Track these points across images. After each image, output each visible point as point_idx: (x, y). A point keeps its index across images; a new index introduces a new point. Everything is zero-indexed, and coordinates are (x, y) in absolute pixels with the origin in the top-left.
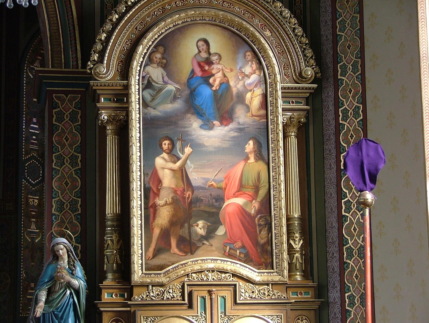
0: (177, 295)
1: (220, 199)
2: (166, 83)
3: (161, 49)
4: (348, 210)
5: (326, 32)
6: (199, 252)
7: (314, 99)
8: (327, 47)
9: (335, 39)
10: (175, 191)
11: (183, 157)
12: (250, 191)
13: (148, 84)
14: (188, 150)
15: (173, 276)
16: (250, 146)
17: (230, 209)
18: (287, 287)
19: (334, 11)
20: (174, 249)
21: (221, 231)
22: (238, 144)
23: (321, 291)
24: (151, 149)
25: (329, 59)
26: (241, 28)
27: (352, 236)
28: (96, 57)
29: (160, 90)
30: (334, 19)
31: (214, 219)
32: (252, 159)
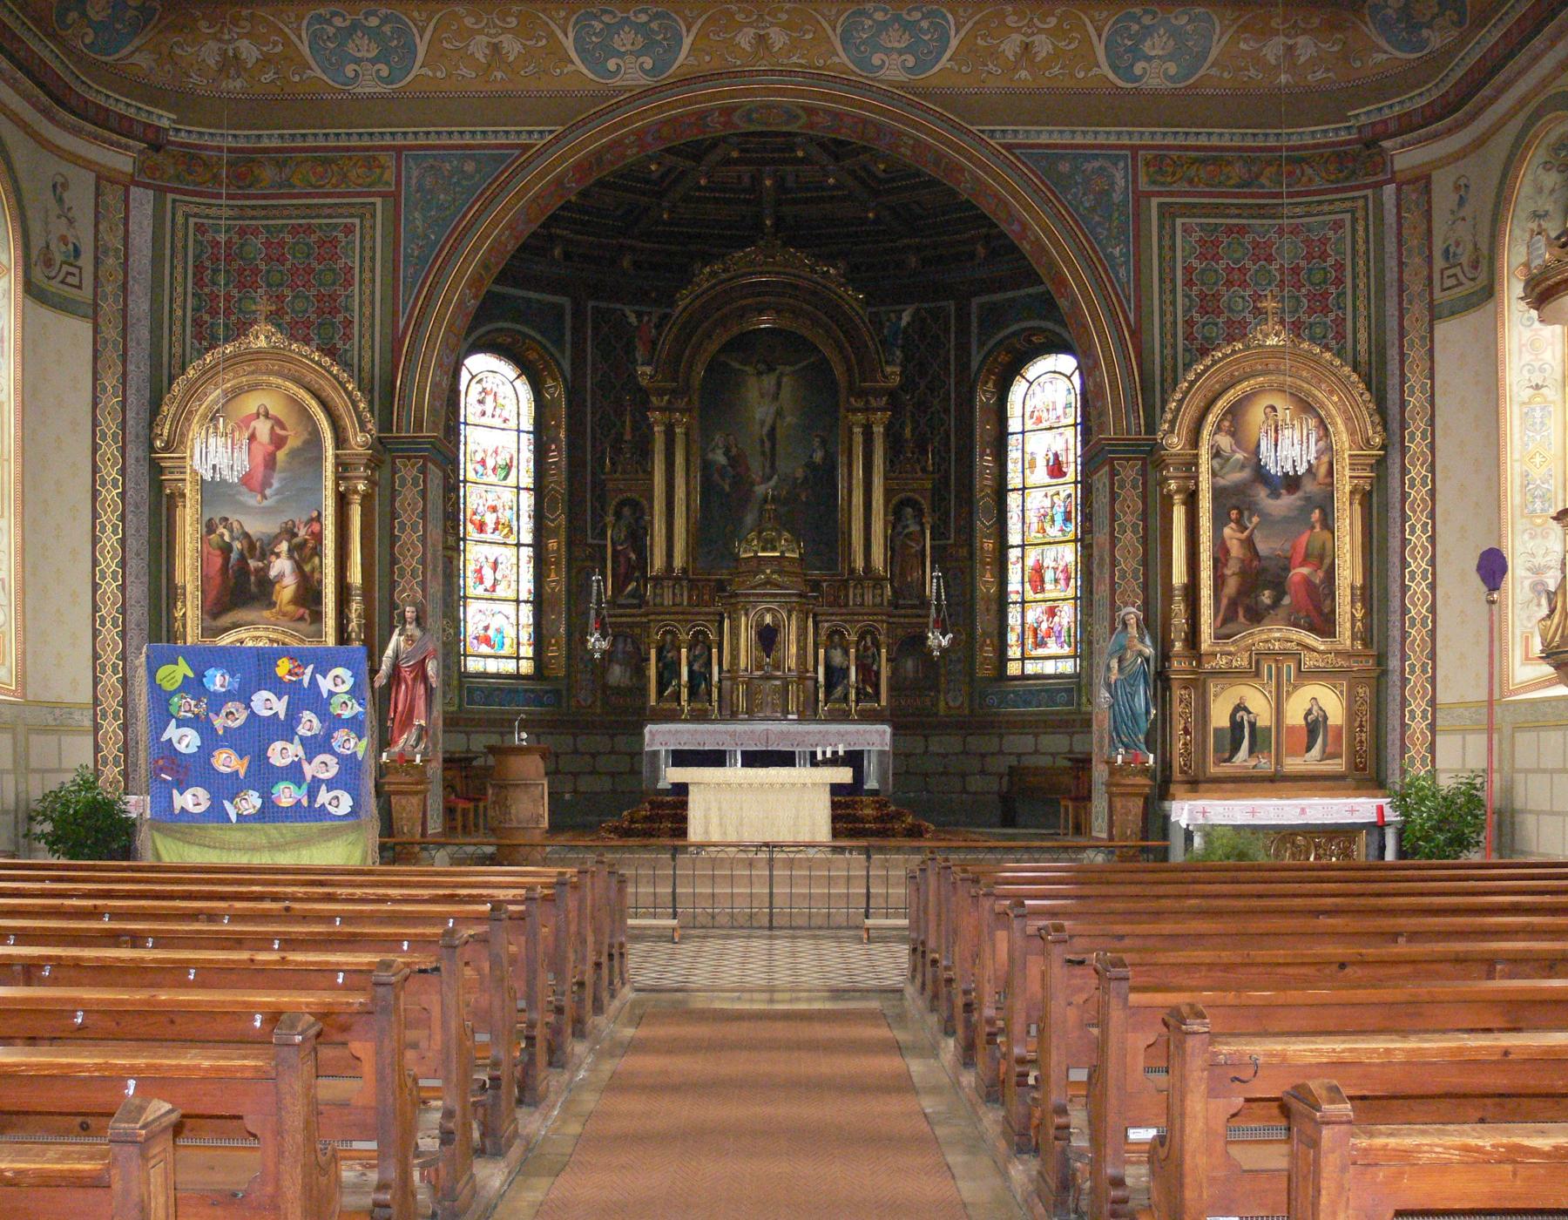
0: (1245, 663)
1: (1287, 569)
2: (1234, 452)
3: (1229, 417)
4: (1412, 579)
5: (1393, 397)
6: (1265, 621)
7: (1381, 464)
8: (1393, 410)
9: (1403, 404)
10: (1243, 561)
11: (1251, 526)
12: (1315, 561)
13: (1217, 453)
14: (1255, 519)
15: (1242, 644)
17: (1296, 579)
18: (1349, 655)
19: (1402, 375)
20: (1241, 619)
21: (1286, 601)
22: (1305, 511)
23: (1381, 659)
24: (1219, 521)
25: (1394, 426)
26: (1309, 394)
27: (1415, 605)
28: (1166, 426)
29: (1228, 459)
30: (1402, 383)
31: (1279, 589)
32: (1318, 529)
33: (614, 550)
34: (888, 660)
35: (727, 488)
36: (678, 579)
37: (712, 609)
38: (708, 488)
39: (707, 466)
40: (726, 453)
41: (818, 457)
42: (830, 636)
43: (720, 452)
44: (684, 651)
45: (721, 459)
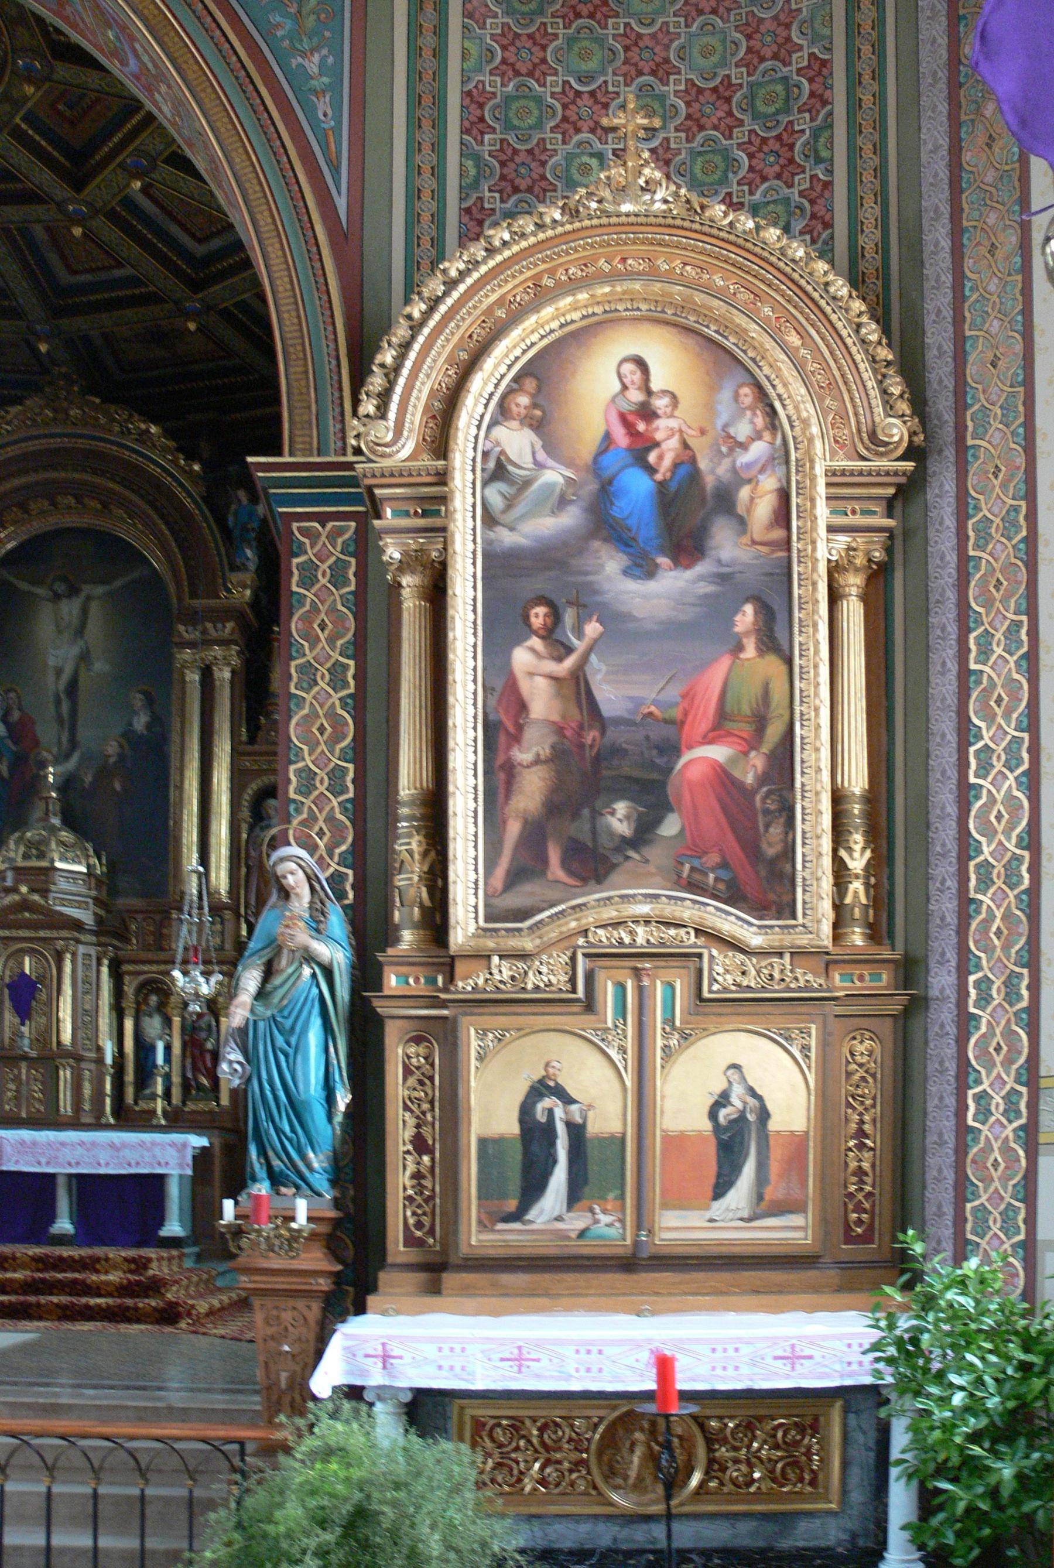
1: (671, 749)
8: (939, 372)
10: (559, 730)
11: (580, 646)
12: (745, 729)
13: (498, 471)
14: (592, 629)
16: (747, 616)
17: (695, 773)
21: (671, 826)
24: (501, 628)
25: (942, 404)
26: (726, 327)
29: (527, 483)
31: (653, 796)
32: (750, 651)
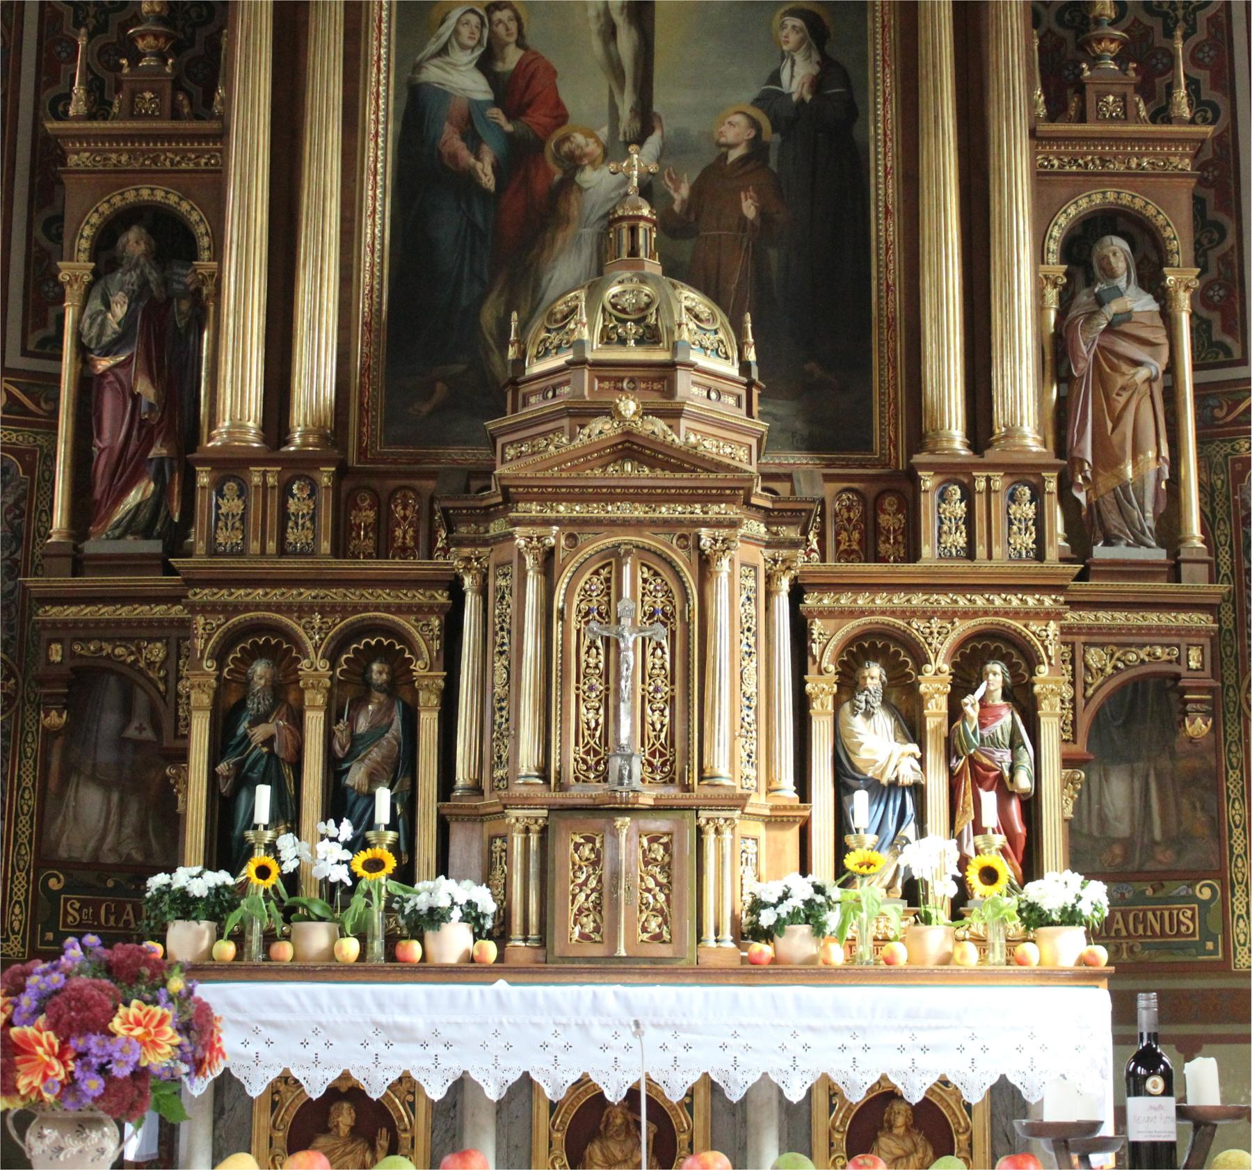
33: (88, 385)
34: (1068, 762)
35: (488, 179)
36: (301, 466)
37: (415, 565)
38: (423, 175)
39: (418, 108)
40: (485, 64)
41: (797, 78)
42: (849, 684)
43: (465, 59)
44: (314, 722)
45: (463, 79)
